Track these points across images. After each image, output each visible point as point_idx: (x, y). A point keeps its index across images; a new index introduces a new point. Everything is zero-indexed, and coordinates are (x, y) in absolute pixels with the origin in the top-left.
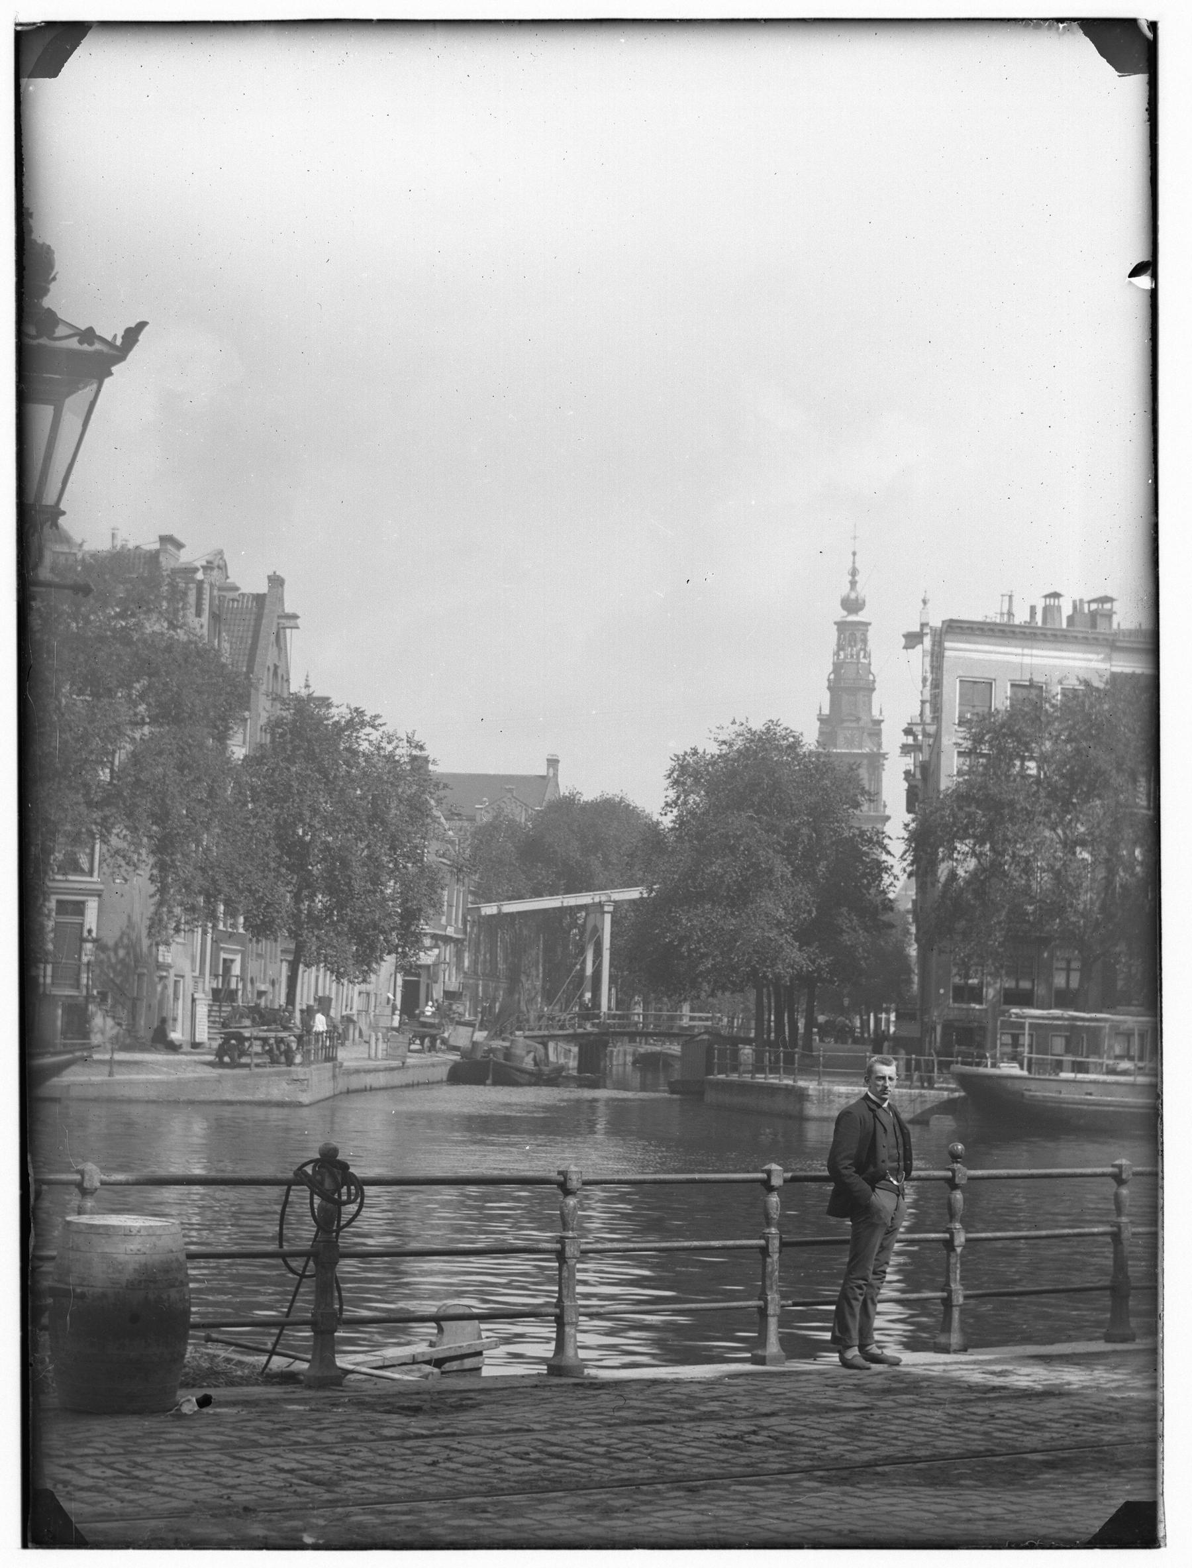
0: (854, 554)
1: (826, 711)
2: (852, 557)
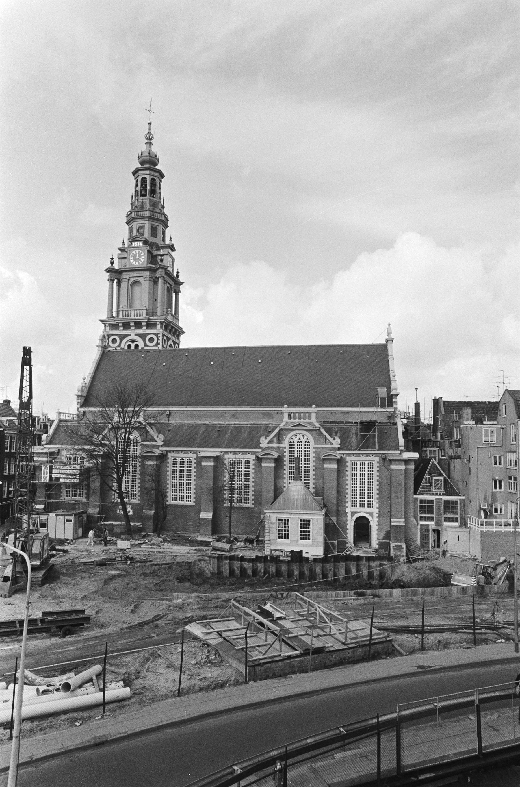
0: (150, 124)
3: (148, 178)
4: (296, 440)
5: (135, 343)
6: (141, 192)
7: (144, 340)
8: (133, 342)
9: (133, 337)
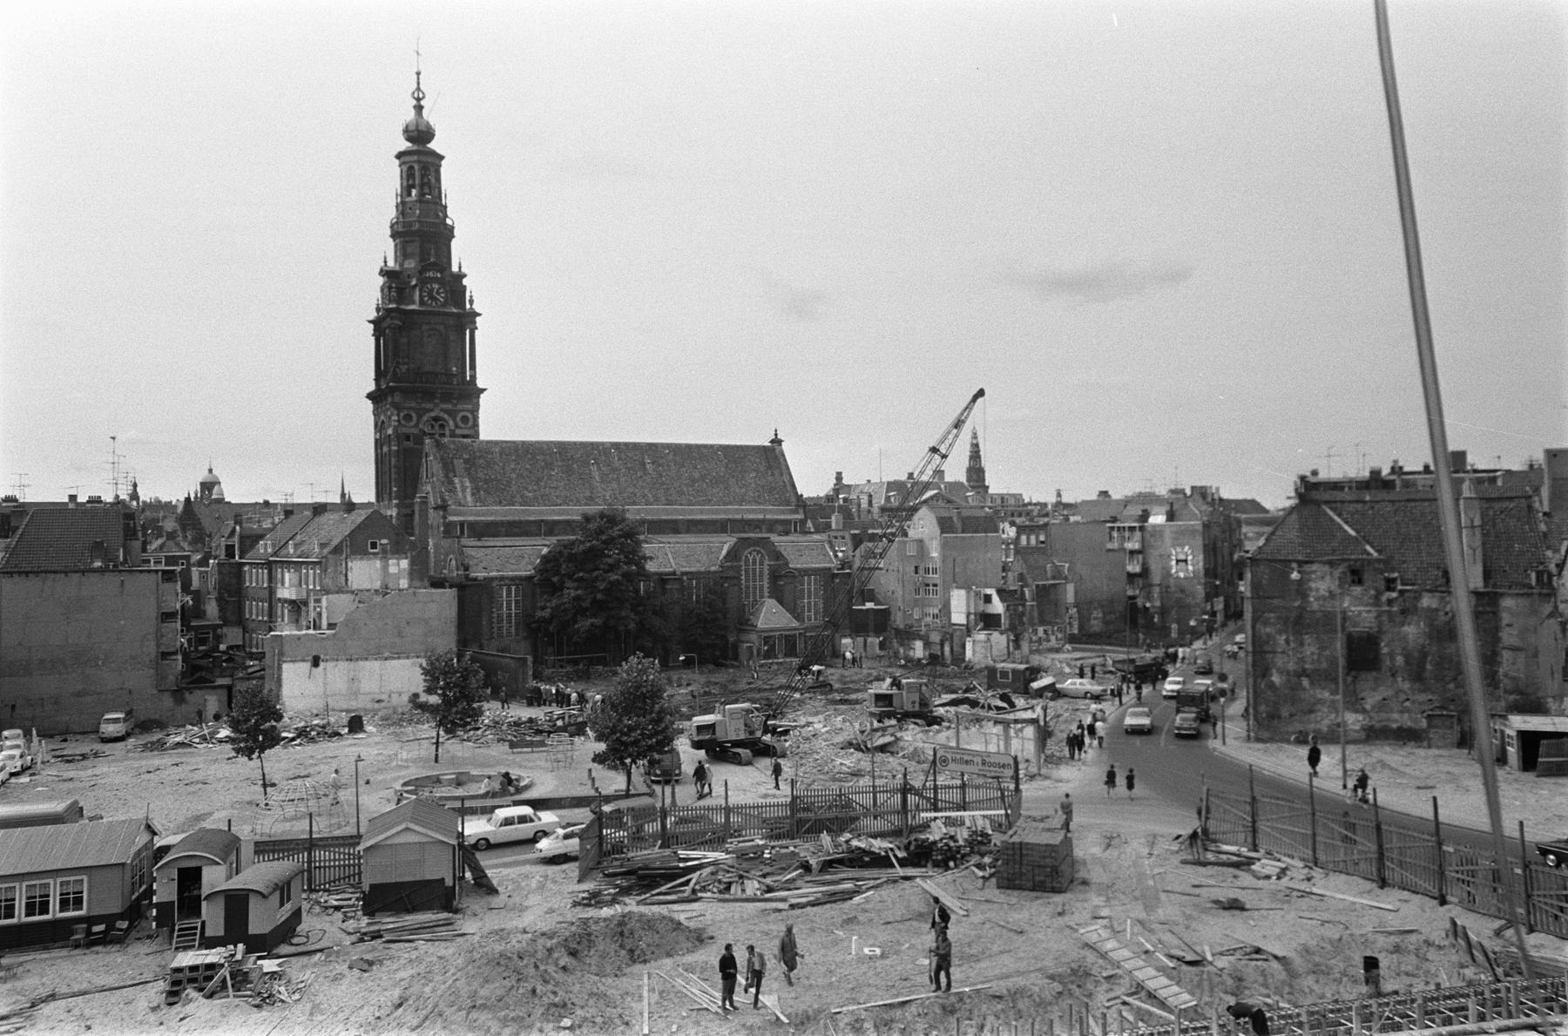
0: (418, 74)
1: (391, 263)
2: (416, 76)
4: (751, 558)
7: (454, 420)
8: (436, 419)
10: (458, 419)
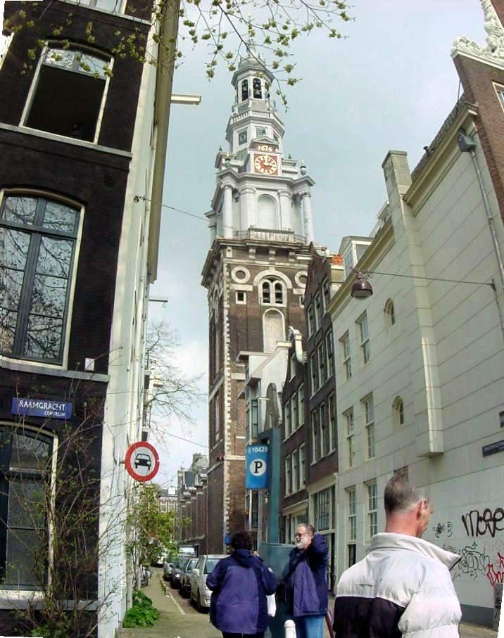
3: (263, 82)
5: (276, 282)
6: (255, 92)
7: (292, 278)
9: (272, 272)
10: (297, 279)
